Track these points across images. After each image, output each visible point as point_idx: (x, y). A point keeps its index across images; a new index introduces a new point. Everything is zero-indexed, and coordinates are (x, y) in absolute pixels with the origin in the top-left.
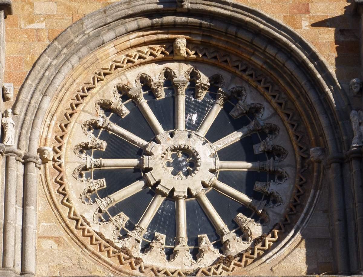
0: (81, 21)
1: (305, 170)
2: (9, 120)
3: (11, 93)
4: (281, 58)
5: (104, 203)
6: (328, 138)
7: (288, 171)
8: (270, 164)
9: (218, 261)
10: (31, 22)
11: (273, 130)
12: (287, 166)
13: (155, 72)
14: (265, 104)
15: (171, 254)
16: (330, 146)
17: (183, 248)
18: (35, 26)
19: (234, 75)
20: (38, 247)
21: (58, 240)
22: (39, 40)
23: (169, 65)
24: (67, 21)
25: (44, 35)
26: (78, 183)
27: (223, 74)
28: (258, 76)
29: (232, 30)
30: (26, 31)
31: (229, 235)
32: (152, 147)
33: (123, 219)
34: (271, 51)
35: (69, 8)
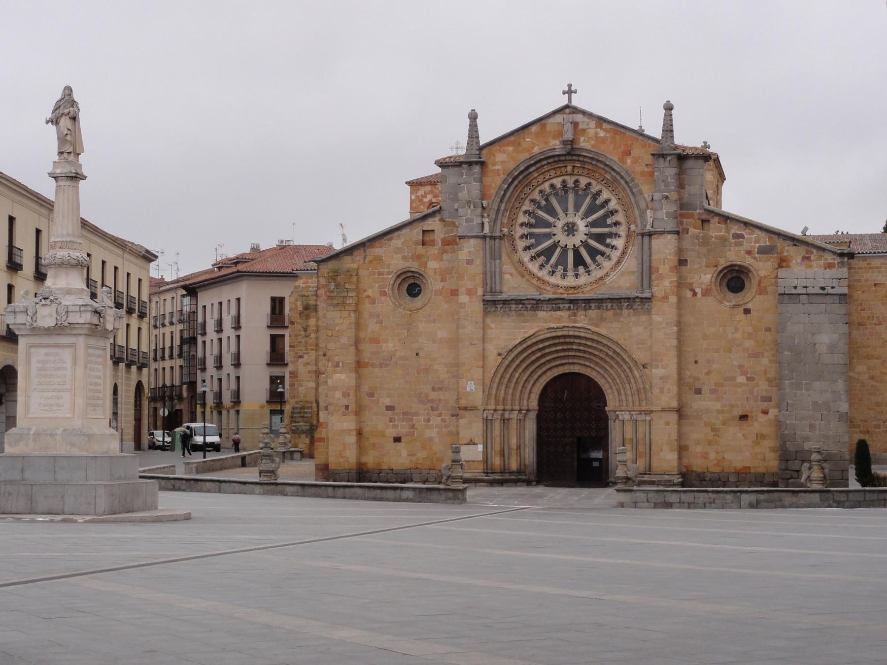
1: (629, 235)
2: (486, 221)
4: (618, 177)
5: (533, 252)
8: (614, 230)
10: (495, 165)
11: (616, 211)
12: (622, 230)
13: (558, 182)
14: (613, 198)
15: (564, 276)
16: (639, 225)
18: (497, 167)
21: (511, 274)
22: (499, 175)
25: (501, 172)
29: (594, 162)
30: (493, 171)
34: (612, 172)
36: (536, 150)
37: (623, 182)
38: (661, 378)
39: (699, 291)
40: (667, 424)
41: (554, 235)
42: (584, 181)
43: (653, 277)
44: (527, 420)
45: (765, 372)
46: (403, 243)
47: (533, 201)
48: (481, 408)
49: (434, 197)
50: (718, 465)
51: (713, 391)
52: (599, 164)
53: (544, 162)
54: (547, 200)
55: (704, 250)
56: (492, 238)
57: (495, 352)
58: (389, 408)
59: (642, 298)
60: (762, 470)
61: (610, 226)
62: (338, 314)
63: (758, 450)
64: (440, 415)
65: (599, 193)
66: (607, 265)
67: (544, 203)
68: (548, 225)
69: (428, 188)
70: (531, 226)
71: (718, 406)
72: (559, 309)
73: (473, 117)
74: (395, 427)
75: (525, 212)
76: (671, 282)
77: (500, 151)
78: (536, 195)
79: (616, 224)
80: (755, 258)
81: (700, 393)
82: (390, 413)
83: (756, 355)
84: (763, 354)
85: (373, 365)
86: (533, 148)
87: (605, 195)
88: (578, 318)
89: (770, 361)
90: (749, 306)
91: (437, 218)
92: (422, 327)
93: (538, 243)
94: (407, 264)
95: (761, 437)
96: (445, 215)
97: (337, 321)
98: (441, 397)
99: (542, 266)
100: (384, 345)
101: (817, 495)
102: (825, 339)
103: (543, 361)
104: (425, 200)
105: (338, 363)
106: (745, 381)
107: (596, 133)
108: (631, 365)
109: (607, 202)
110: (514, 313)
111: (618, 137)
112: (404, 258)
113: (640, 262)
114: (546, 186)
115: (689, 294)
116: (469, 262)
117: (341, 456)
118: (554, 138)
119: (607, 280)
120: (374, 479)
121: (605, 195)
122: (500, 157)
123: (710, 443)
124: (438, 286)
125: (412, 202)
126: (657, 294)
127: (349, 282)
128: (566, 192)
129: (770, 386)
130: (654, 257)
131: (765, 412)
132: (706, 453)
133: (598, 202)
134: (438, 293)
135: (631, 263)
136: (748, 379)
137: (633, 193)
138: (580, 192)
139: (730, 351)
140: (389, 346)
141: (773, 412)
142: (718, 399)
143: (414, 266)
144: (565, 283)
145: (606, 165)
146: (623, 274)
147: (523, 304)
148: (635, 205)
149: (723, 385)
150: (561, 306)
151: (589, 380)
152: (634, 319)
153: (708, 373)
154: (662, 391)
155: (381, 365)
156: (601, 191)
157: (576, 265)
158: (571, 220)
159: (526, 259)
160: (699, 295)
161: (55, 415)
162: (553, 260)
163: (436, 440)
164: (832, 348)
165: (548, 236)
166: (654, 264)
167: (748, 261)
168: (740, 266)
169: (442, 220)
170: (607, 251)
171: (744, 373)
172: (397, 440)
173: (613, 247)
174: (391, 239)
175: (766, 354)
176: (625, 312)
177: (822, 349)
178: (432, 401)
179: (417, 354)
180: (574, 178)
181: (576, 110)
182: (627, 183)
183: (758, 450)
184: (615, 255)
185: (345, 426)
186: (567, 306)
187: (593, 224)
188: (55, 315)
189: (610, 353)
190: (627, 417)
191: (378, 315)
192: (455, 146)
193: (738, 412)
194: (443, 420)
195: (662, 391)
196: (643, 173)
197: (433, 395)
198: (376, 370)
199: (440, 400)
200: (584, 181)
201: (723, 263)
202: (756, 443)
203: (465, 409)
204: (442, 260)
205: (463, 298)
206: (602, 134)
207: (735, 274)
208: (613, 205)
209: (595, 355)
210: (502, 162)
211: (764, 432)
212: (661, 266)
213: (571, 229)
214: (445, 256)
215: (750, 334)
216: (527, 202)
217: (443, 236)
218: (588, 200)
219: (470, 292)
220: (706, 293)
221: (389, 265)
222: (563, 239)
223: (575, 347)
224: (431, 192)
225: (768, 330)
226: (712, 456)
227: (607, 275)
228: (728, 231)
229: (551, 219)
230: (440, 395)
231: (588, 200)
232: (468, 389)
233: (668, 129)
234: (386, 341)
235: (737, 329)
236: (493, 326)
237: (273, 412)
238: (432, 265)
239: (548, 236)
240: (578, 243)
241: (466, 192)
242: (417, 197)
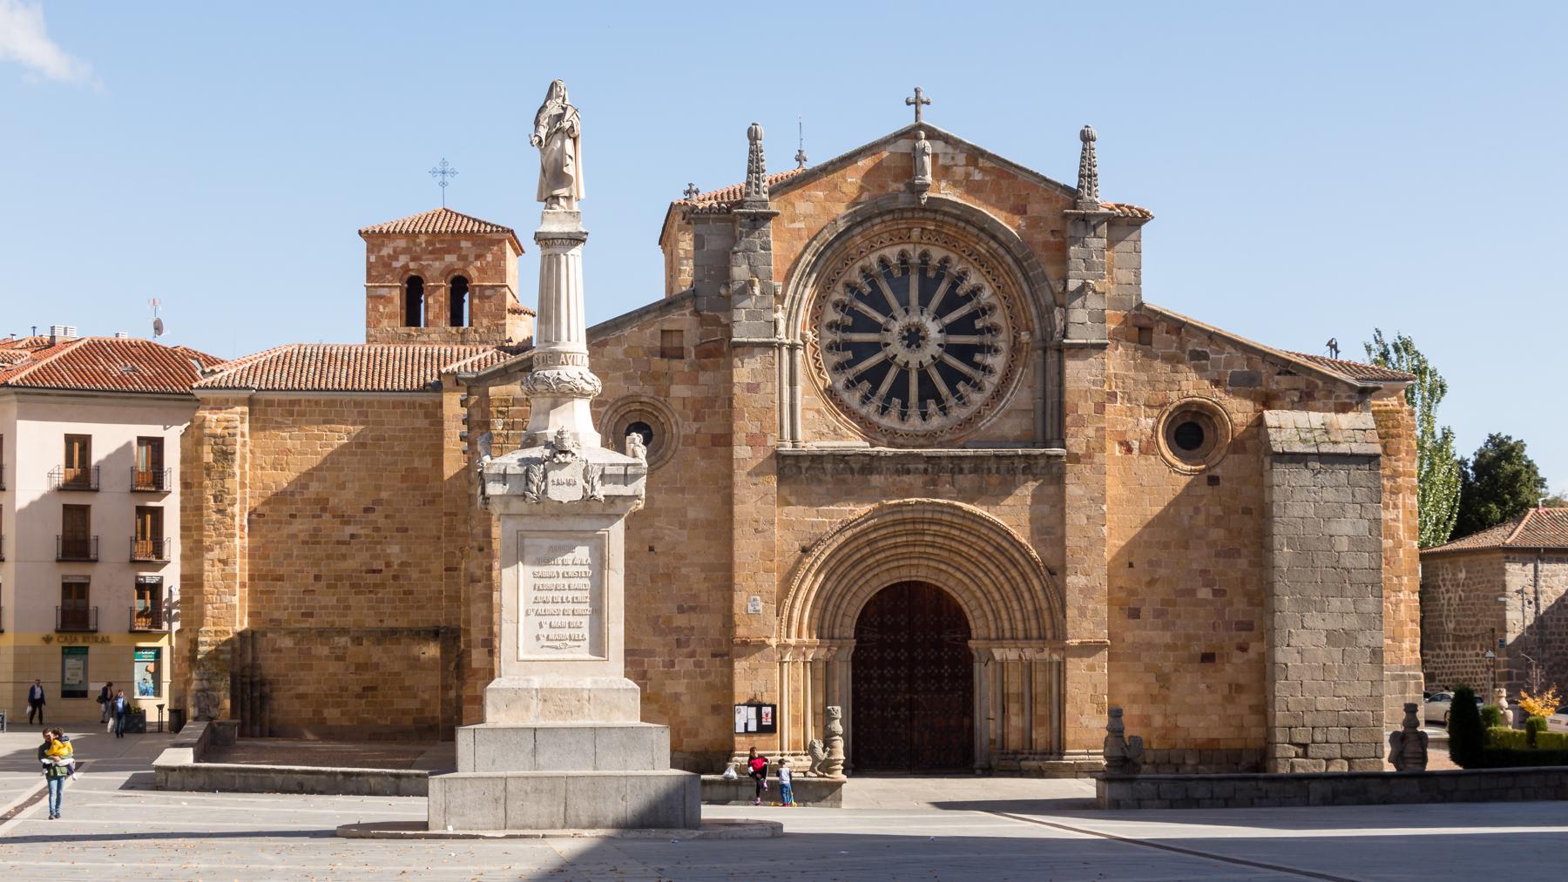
0: (835, 221)
1: (1015, 348)
2: (780, 316)
3: (780, 291)
4: (1001, 251)
5: (851, 373)
6: (1037, 327)
7: (1003, 345)
11: (992, 308)
12: (1002, 341)
13: (892, 253)
15: (903, 416)
16: (1038, 332)
17: (914, 412)
18: (797, 225)
19: (961, 257)
20: (803, 418)
21: (818, 411)
23: (906, 247)
24: (823, 221)
25: (805, 233)
26: (830, 356)
27: (952, 256)
28: (981, 261)
29: (962, 224)
31: (952, 401)
33: (866, 385)
34: (994, 244)
37: (1009, 259)
38: (1081, 591)
39: (1135, 445)
41: (887, 345)
42: (937, 254)
43: (1068, 419)
44: (838, 664)
45: (1243, 582)
46: (626, 352)
47: (851, 287)
48: (773, 642)
49: (414, 259)
50: (1163, 737)
51: (1159, 614)
52: (969, 228)
53: (878, 220)
54: (873, 284)
55: (1144, 377)
56: (793, 348)
59: (1049, 457)
60: (1238, 745)
61: (980, 332)
63: (1231, 710)
64: (692, 655)
65: (962, 277)
66: (977, 398)
67: (867, 290)
68: (876, 327)
69: (402, 243)
70: (846, 329)
71: (1167, 637)
72: (908, 472)
73: (753, 136)
75: (836, 305)
76: (1097, 430)
77: (801, 196)
78: (855, 276)
79: (993, 329)
80: (1227, 392)
81: (1138, 617)
83: (1230, 553)
84: (1238, 551)
87: (973, 279)
88: (939, 489)
89: (1251, 564)
90: (1218, 471)
91: (687, 312)
93: (858, 358)
94: (635, 389)
95: (1236, 688)
96: (703, 303)
98: (694, 624)
99: (865, 400)
101: (1415, 781)
102: (1347, 527)
103: (870, 561)
104: (396, 264)
106: (1210, 597)
107: (968, 175)
108: (1028, 570)
109: (976, 291)
110: (829, 478)
111: (1004, 183)
112: (627, 378)
113: (1039, 394)
114: (873, 259)
115: (1117, 450)
116: (752, 388)
118: (896, 180)
119: (983, 425)
120: (340, 777)
121: (973, 279)
122: (802, 207)
123: (1153, 699)
124: (690, 428)
125: (370, 267)
126: (1074, 450)
128: (905, 271)
129: (1251, 604)
130: (1070, 385)
131: (1243, 648)
132: (1148, 717)
133: (961, 291)
134: (690, 440)
135: (1020, 395)
136: (1216, 593)
137: (1027, 278)
138: (930, 276)
142: (1166, 627)
143: (646, 391)
144: (906, 427)
145: (982, 230)
146: (1008, 415)
148: (1030, 299)
149: (1174, 604)
150: (911, 466)
151: (939, 591)
154: (1082, 612)
156: (965, 273)
157: (922, 399)
158: (916, 320)
160: (1136, 452)
161: (570, 657)
162: (884, 388)
163: (685, 699)
164: (1357, 543)
165: (876, 347)
166: (1069, 399)
168: (1201, 405)
169: (696, 312)
170: (978, 376)
171: (1208, 584)
173: (987, 370)
175: (1244, 551)
178: (679, 629)
179: (651, 549)
181: (933, 135)
182: (1016, 260)
183: (1231, 710)
184: (991, 382)
187: (949, 329)
188: (581, 482)
189: (990, 549)
190: (1012, 655)
192: (448, 168)
193: (1198, 648)
194: (698, 664)
196: (1046, 245)
197: (681, 621)
199: (692, 628)
200: (937, 254)
201: (1175, 398)
202: (1229, 699)
204: (696, 384)
205: (741, 451)
206: (977, 176)
207: (1188, 419)
208: (986, 296)
209: (959, 553)
211: (1242, 681)
212: (1082, 403)
213: (914, 337)
214: (705, 377)
215: (1218, 519)
216: (840, 287)
218: (943, 288)
219: (754, 441)
220: (1149, 448)
222: (898, 350)
223: (928, 538)
224: (407, 251)
225: (1247, 511)
226: (1158, 721)
227: (979, 415)
229: (881, 319)
230: (694, 620)
231: (943, 288)
232: (750, 608)
233: (1087, 174)
235: (1197, 510)
237: (68, 652)
238: (679, 391)
239: (876, 347)
240: (927, 360)
241: (745, 267)
242: (380, 258)
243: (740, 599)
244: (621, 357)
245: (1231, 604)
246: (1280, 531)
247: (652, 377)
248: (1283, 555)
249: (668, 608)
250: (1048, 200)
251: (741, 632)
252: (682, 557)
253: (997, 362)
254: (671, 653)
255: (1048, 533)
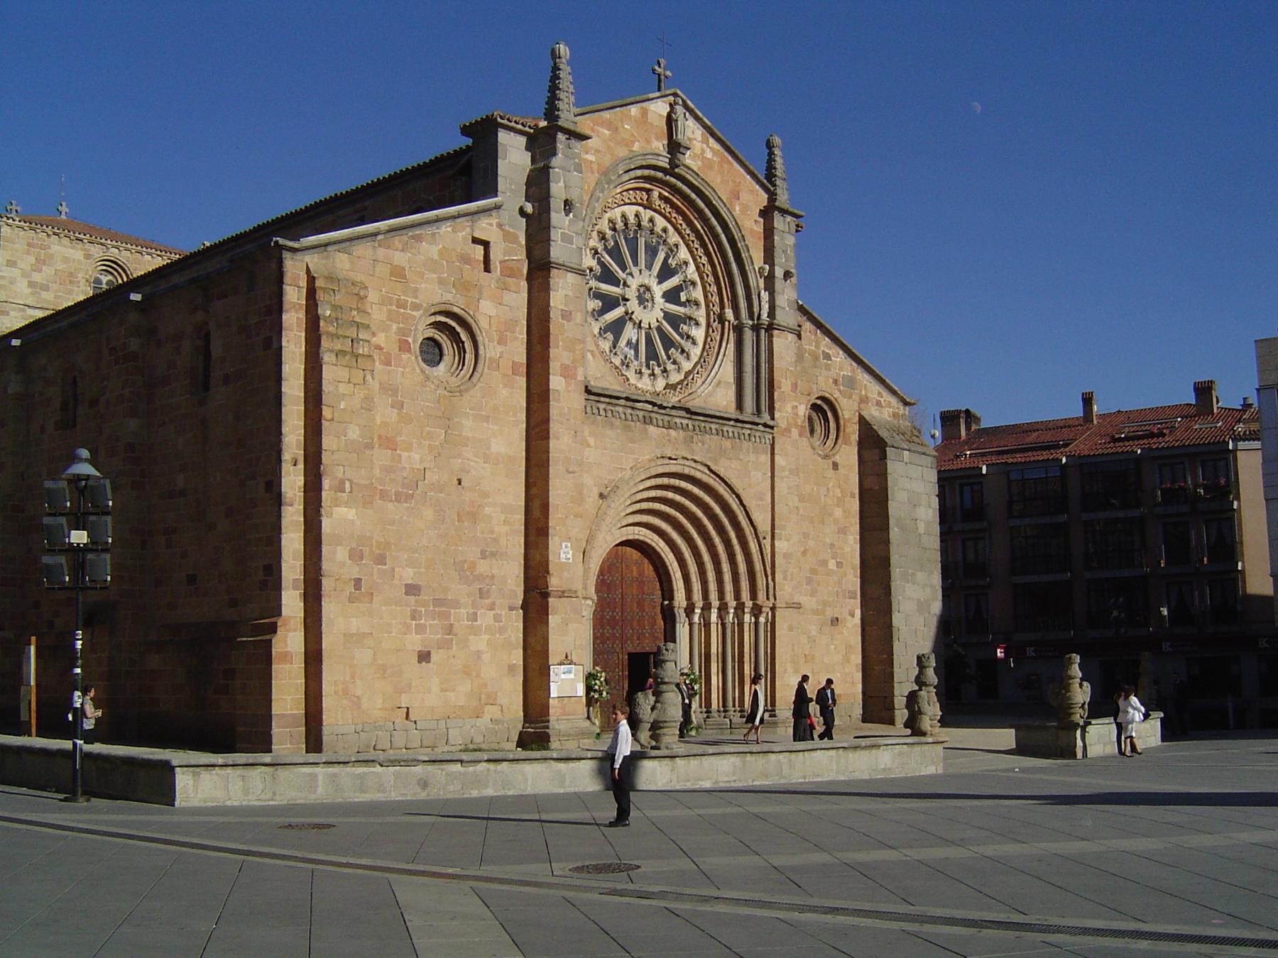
9: (667, 386)
12: (701, 314)
18: (590, 157)
25: (595, 167)
31: (670, 367)
32: (630, 280)
35: (609, 146)
36: (636, 147)
38: (785, 556)
40: (791, 629)
57: (596, 492)
58: (412, 589)
62: (344, 373)
64: (492, 607)
74: (420, 629)
82: (412, 598)
85: (384, 495)
86: (633, 142)
90: (837, 458)
91: (494, 221)
92: (468, 427)
94: (448, 297)
97: (343, 388)
98: (495, 571)
100: (405, 454)
105: (342, 482)
107: (703, 151)
112: (441, 282)
116: (566, 315)
117: (346, 692)
127: (358, 309)
136: (839, 565)
139: (823, 522)
140: (414, 458)
141: (858, 612)
142: (813, 593)
147: (633, 408)
152: (752, 457)
153: (804, 553)
154: (785, 579)
155: (398, 498)
158: (646, 282)
159: (596, 331)
163: (486, 657)
167: (837, 395)
170: (687, 345)
172: (424, 657)
174: (419, 239)
176: (745, 444)
177: (922, 527)
178: (480, 578)
180: (649, 213)
184: (696, 352)
185: (355, 625)
186: (685, 422)
191: (395, 391)
193: (830, 613)
194: (497, 618)
195: (785, 579)
197: (483, 567)
198: (390, 505)
199: (493, 577)
203: (562, 594)
206: (709, 155)
210: (597, 151)
214: (508, 297)
217: (501, 257)
219: (567, 373)
221: (416, 290)
228: (817, 346)
231: (661, 256)
232: (563, 556)
234: (409, 448)
236: (591, 441)
241: (561, 184)
243: (553, 542)
244: (436, 257)
245: (845, 575)
246: (894, 508)
247: (465, 287)
248: (894, 533)
249: (472, 553)
250: (752, 191)
251: (554, 582)
252: (485, 495)
253: (699, 333)
254: (474, 605)
255: (762, 500)
